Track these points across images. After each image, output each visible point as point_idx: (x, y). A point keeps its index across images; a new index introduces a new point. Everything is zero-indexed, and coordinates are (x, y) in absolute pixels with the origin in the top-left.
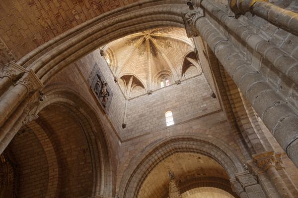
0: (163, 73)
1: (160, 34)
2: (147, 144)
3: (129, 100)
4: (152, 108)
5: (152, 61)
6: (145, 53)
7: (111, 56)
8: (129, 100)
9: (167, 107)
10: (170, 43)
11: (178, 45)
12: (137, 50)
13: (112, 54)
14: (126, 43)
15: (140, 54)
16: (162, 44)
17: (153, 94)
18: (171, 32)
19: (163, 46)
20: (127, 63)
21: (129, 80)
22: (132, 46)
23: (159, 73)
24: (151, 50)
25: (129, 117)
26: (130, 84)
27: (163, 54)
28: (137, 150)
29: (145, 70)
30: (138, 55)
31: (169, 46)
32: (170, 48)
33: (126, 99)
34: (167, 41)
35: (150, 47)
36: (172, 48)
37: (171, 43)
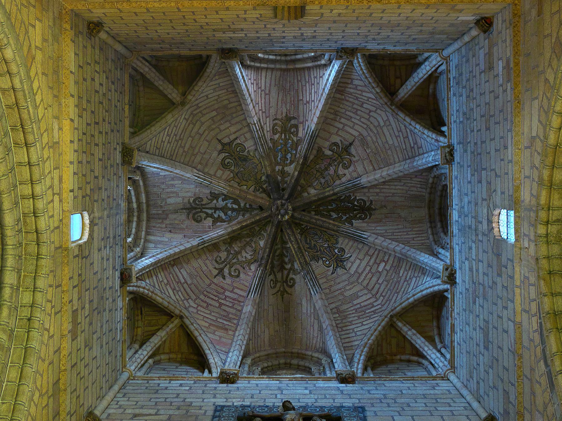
0: (437, 206)
1: (293, 166)
2: (539, 350)
3: (453, 368)
4: (479, 284)
5: (380, 229)
6: (343, 242)
7: (295, 362)
8: (453, 368)
9: (485, 223)
10: (335, 144)
11: (349, 119)
12: (319, 267)
13: (293, 355)
14: (283, 292)
15: (340, 262)
16: (332, 170)
17: (457, 266)
18: (301, 129)
19: (341, 171)
20: (346, 317)
21: (399, 332)
22: (297, 278)
23: (432, 221)
24: (339, 219)
25: (482, 392)
26: (419, 342)
27: (364, 180)
28: (545, 406)
29: (396, 268)
30: (340, 271)
31: (347, 149)
32: (353, 150)
33: (444, 378)
34: (328, 153)
35: (323, 216)
36: (357, 143)
37: (336, 139)
